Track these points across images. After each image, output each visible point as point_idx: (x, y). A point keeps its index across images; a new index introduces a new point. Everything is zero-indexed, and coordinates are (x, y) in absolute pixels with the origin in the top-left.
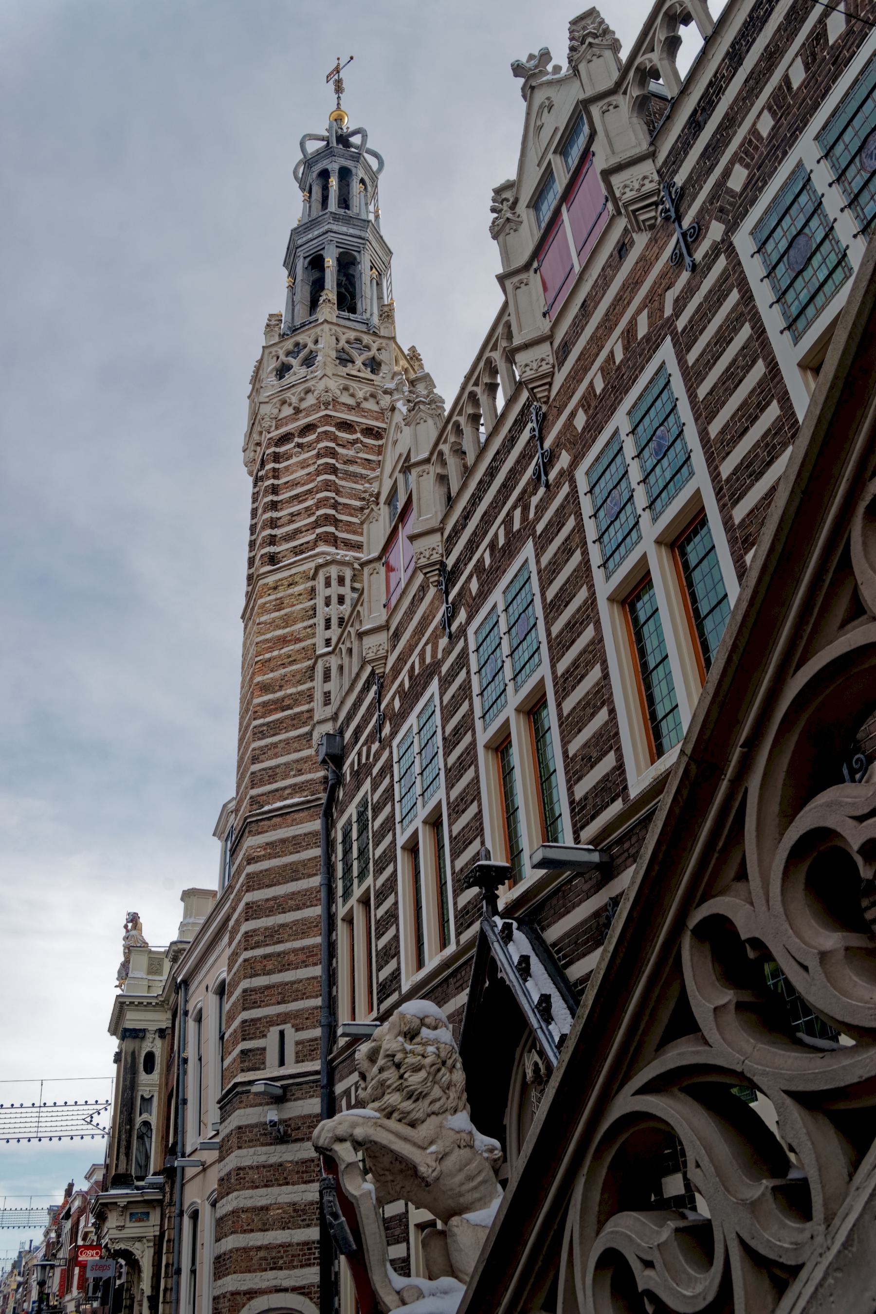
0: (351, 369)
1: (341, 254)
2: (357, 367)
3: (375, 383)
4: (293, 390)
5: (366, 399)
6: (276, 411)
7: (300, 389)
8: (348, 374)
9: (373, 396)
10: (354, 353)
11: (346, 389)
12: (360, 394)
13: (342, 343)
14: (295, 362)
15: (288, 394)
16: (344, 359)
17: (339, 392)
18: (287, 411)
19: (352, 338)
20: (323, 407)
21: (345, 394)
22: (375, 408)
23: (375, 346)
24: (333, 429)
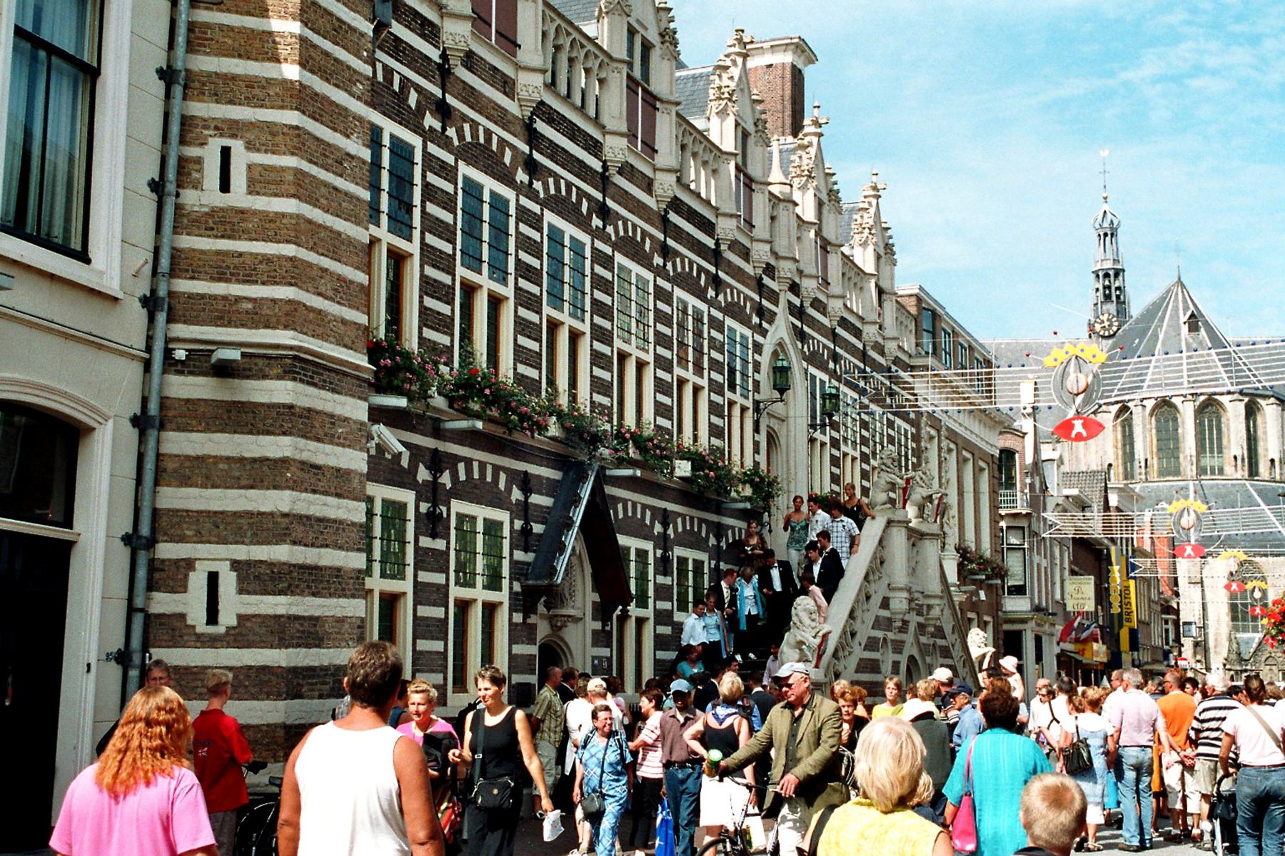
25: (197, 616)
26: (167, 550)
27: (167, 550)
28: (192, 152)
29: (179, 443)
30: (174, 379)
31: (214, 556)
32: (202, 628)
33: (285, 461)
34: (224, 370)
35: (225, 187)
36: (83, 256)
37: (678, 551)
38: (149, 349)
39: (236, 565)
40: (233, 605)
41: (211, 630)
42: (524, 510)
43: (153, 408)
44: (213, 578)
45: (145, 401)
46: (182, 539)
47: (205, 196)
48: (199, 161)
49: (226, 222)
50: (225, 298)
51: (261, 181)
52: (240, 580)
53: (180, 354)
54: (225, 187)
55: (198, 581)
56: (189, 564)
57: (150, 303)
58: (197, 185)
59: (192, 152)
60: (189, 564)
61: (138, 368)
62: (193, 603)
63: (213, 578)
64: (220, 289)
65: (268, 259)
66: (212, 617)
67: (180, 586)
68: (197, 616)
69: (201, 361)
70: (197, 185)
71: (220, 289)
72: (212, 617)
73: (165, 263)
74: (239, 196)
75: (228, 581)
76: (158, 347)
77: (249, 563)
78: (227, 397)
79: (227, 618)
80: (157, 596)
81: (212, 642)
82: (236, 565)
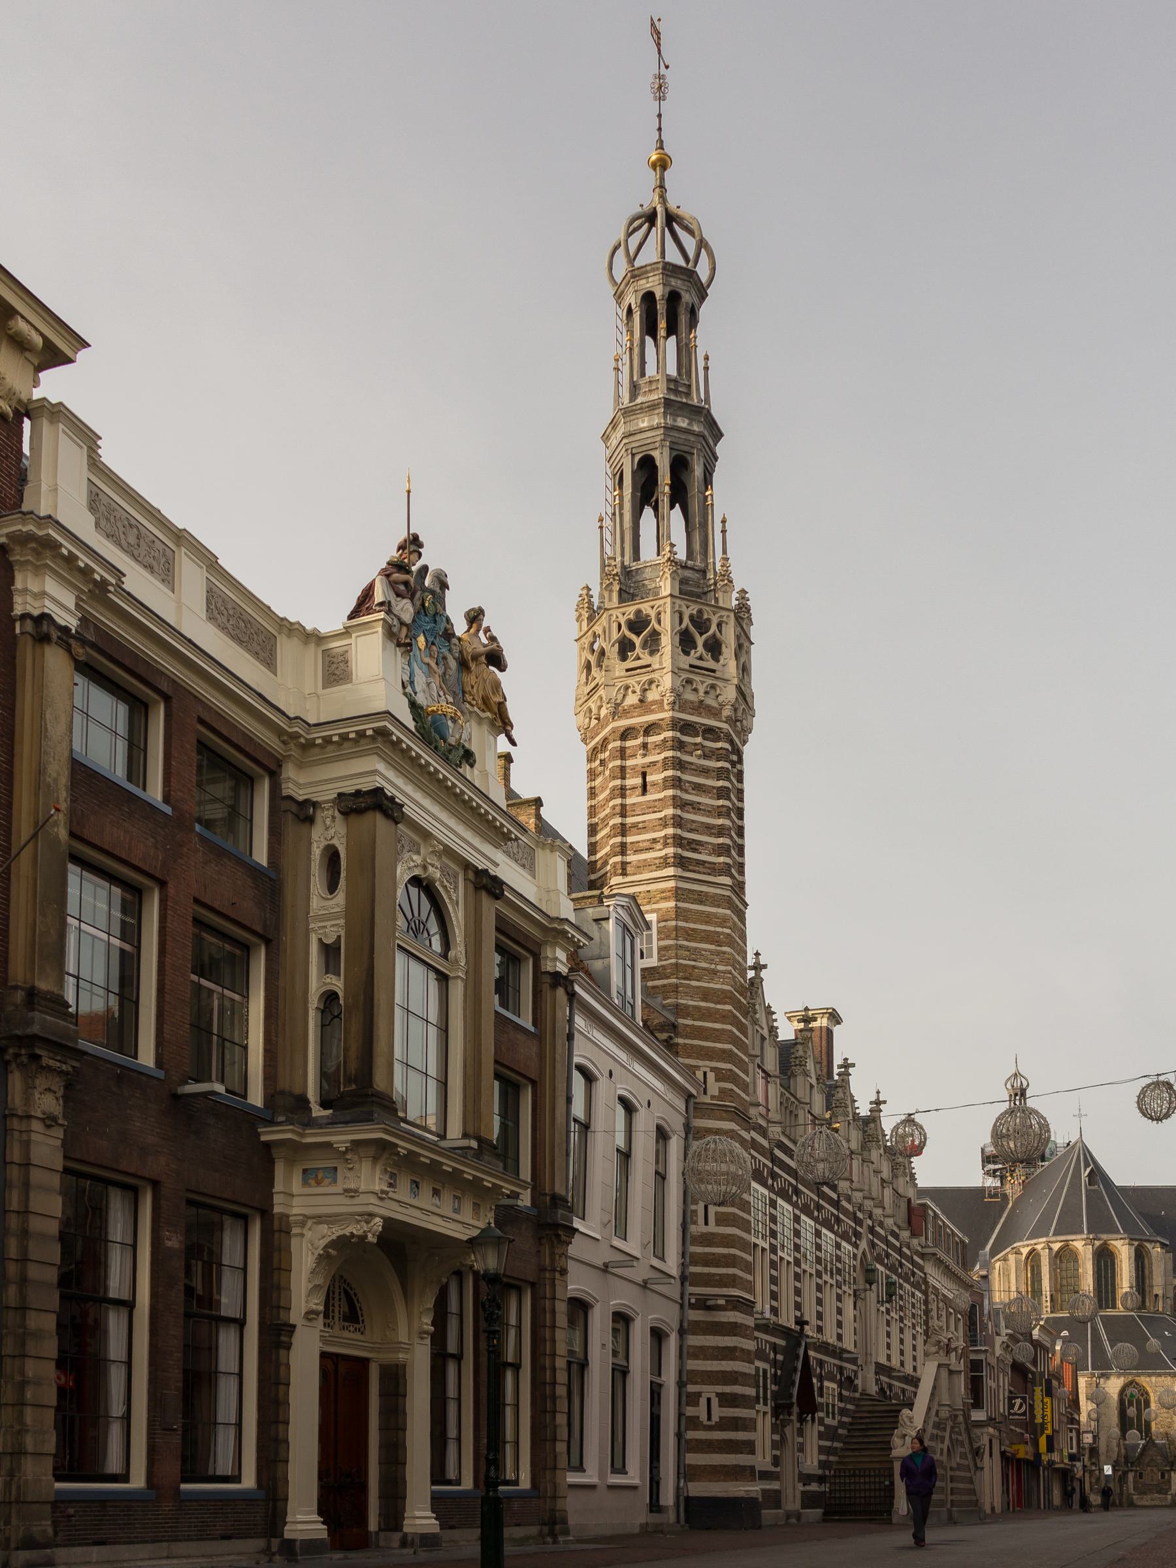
0: (692, 659)
1: (675, 453)
2: (698, 654)
3: (718, 674)
4: (637, 679)
5: (706, 693)
6: (620, 696)
7: (645, 678)
8: (691, 666)
9: (713, 687)
10: (697, 635)
11: (689, 681)
12: (702, 690)
13: (686, 621)
14: (637, 641)
15: (631, 681)
16: (686, 642)
17: (681, 689)
18: (632, 699)
19: (695, 612)
20: (666, 707)
21: (689, 688)
22: (714, 704)
23: (715, 620)
24: (678, 735)
25: (703, 1417)
26: (691, 1388)
27: (691, 1388)
28: (693, 1207)
29: (694, 1340)
30: (691, 1312)
31: (709, 1391)
32: (706, 1422)
33: (735, 1348)
34: (709, 1308)
35: (706, 1223)
36: (662, 1259)
37: (826, 1383)
38: (682, 1298)
39: (718, 1395)
40: (718, 1412)
41: (709, 1423)
42: (774, 1363)
43: (685, 1324)
44: (709, 1400)
45: (681, 1322)
46: (696, 1383)
47: (698, 1228)
48: (695, 1212)
49: (707, 1239)
50: (708, 1274)
51: (722, 1220)
52: (720, 1401)
53: (693, 1301)
54: (706, 1223)
55: (703, 1402)
56: (699, 1394)
57: (683, 1278)
58: (695, 1223)
59: (693, 1207)
60: (699, 1394)
61: (677, 1307)
62: (701, 1411)
63: (709, 1400)
64: (706, 1270)
65: (724, 1256)
66: (709, 1419)
67: (697, 1404)
68: (703, 1417)
69: (703, 1304)
70: (695, 1223)
71: (706, 1270)
72: (709, 1419)
73: (688, 1260)
74: (712, 1228)
75: (715, 1402)
76: (686, 1298)
77: (723, 1394)
78: (710, 1319)
79: (715, 1418)
80: (689, 1408)
81: (710, 1428)
82: (718, 1395)
